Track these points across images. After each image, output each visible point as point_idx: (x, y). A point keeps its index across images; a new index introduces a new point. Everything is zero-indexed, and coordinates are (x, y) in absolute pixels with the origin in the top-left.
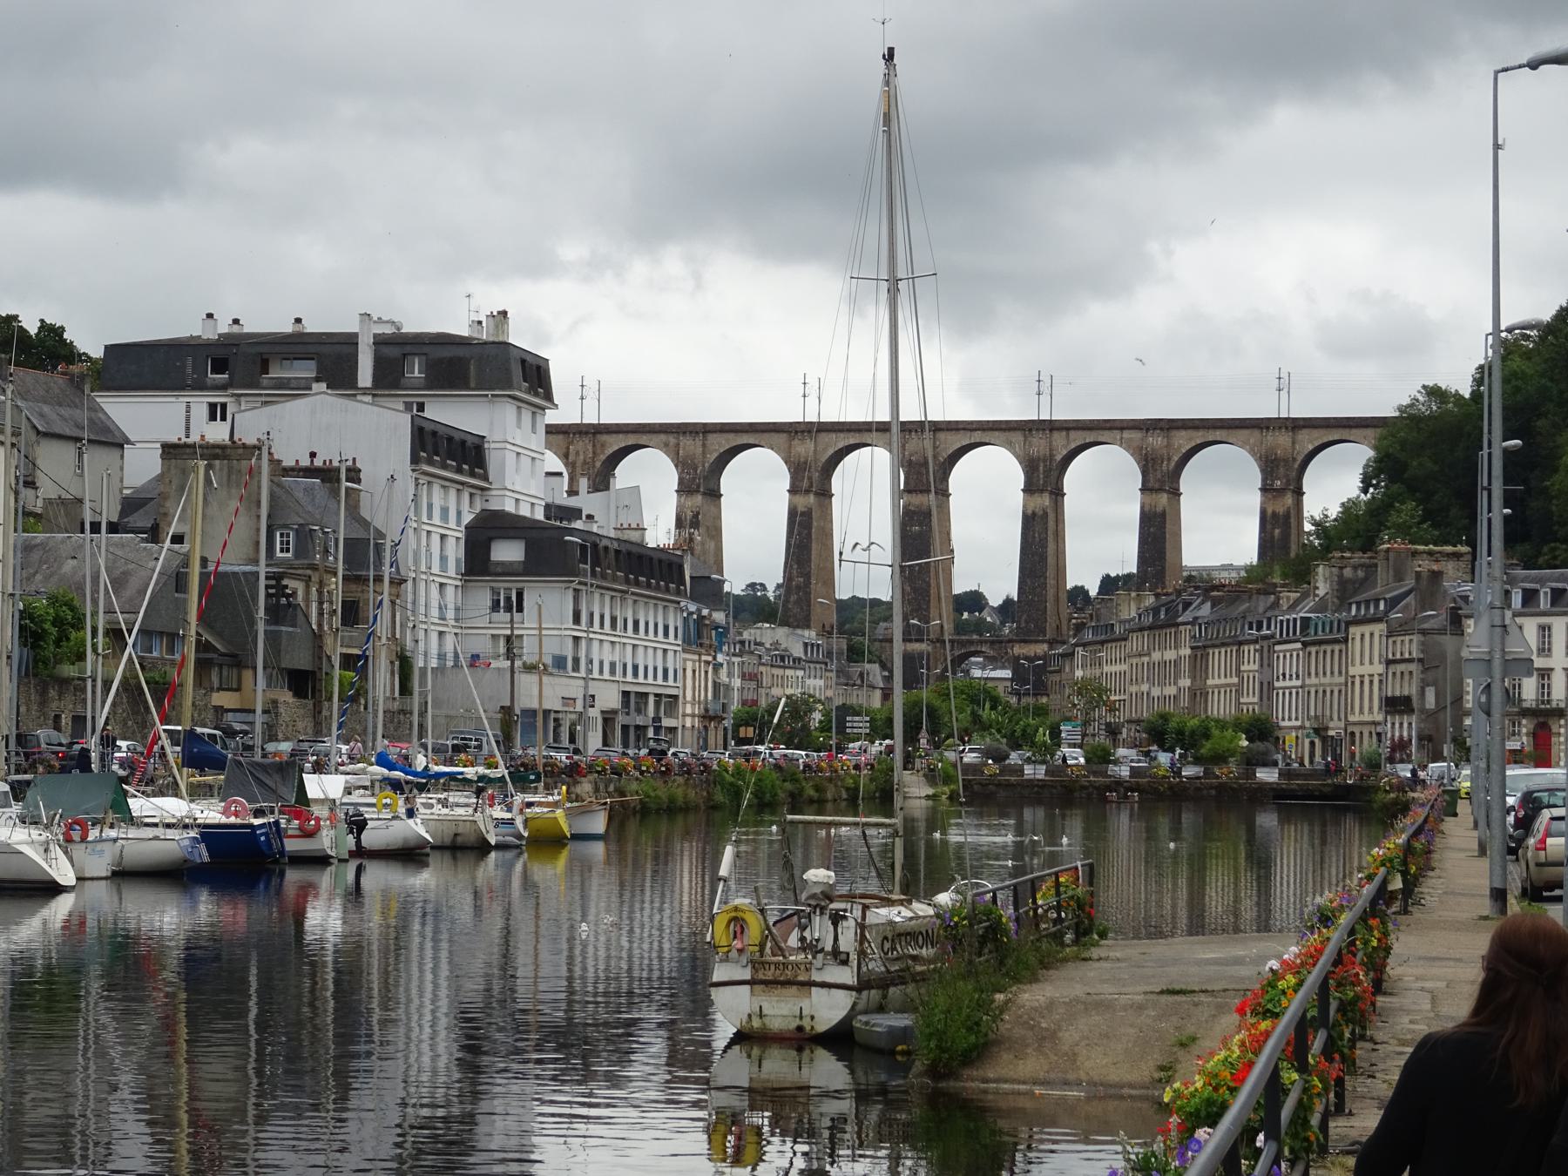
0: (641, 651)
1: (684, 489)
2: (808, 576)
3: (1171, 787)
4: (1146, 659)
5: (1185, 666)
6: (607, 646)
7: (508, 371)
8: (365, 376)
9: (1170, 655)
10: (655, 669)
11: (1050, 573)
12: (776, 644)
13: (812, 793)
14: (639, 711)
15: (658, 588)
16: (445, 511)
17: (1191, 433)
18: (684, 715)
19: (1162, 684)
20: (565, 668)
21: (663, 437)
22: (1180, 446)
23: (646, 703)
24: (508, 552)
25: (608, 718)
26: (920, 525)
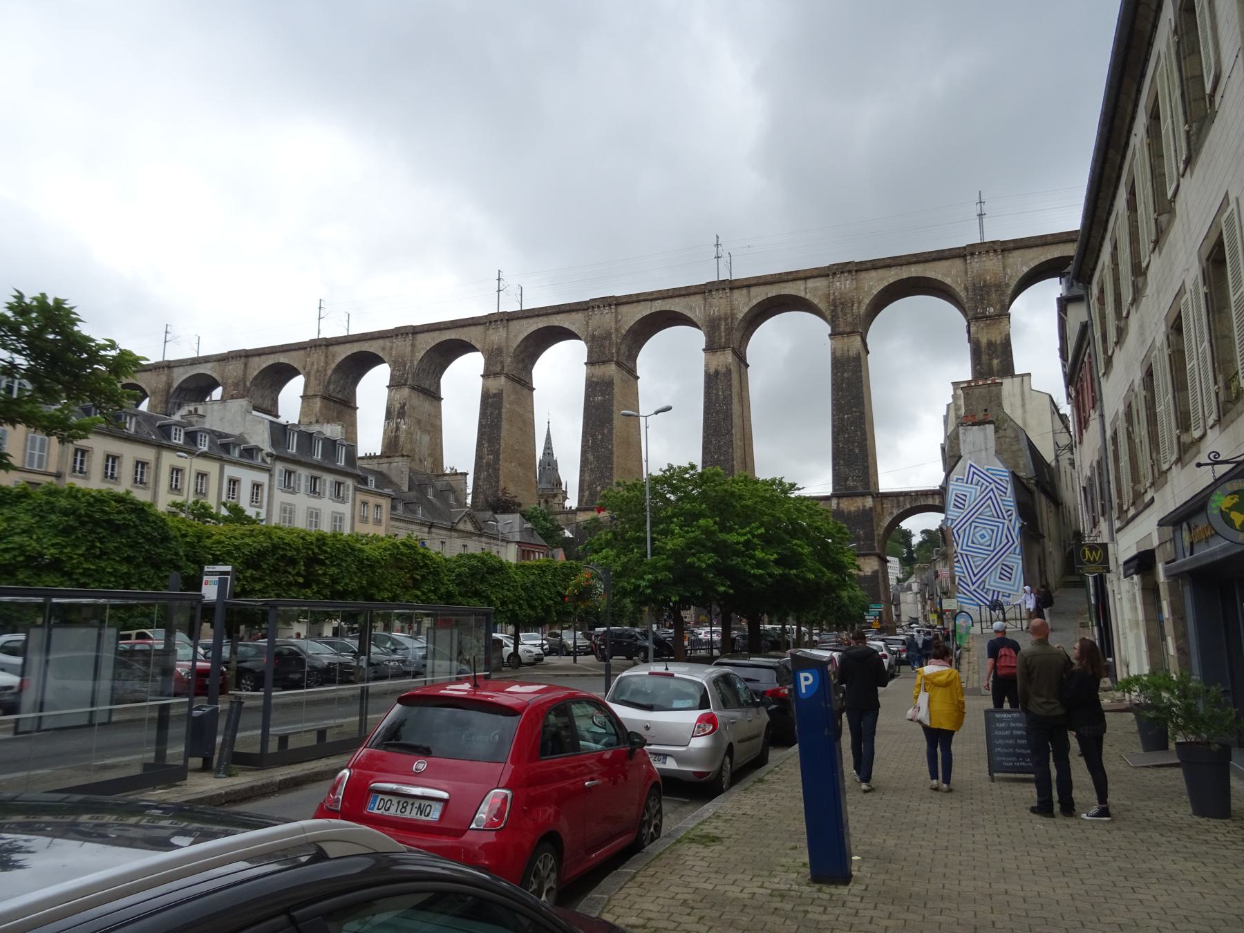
2: (496, 453)
11: (736, 431)
17: (880, 271)
22: (871, 288)
26: (603, 395)
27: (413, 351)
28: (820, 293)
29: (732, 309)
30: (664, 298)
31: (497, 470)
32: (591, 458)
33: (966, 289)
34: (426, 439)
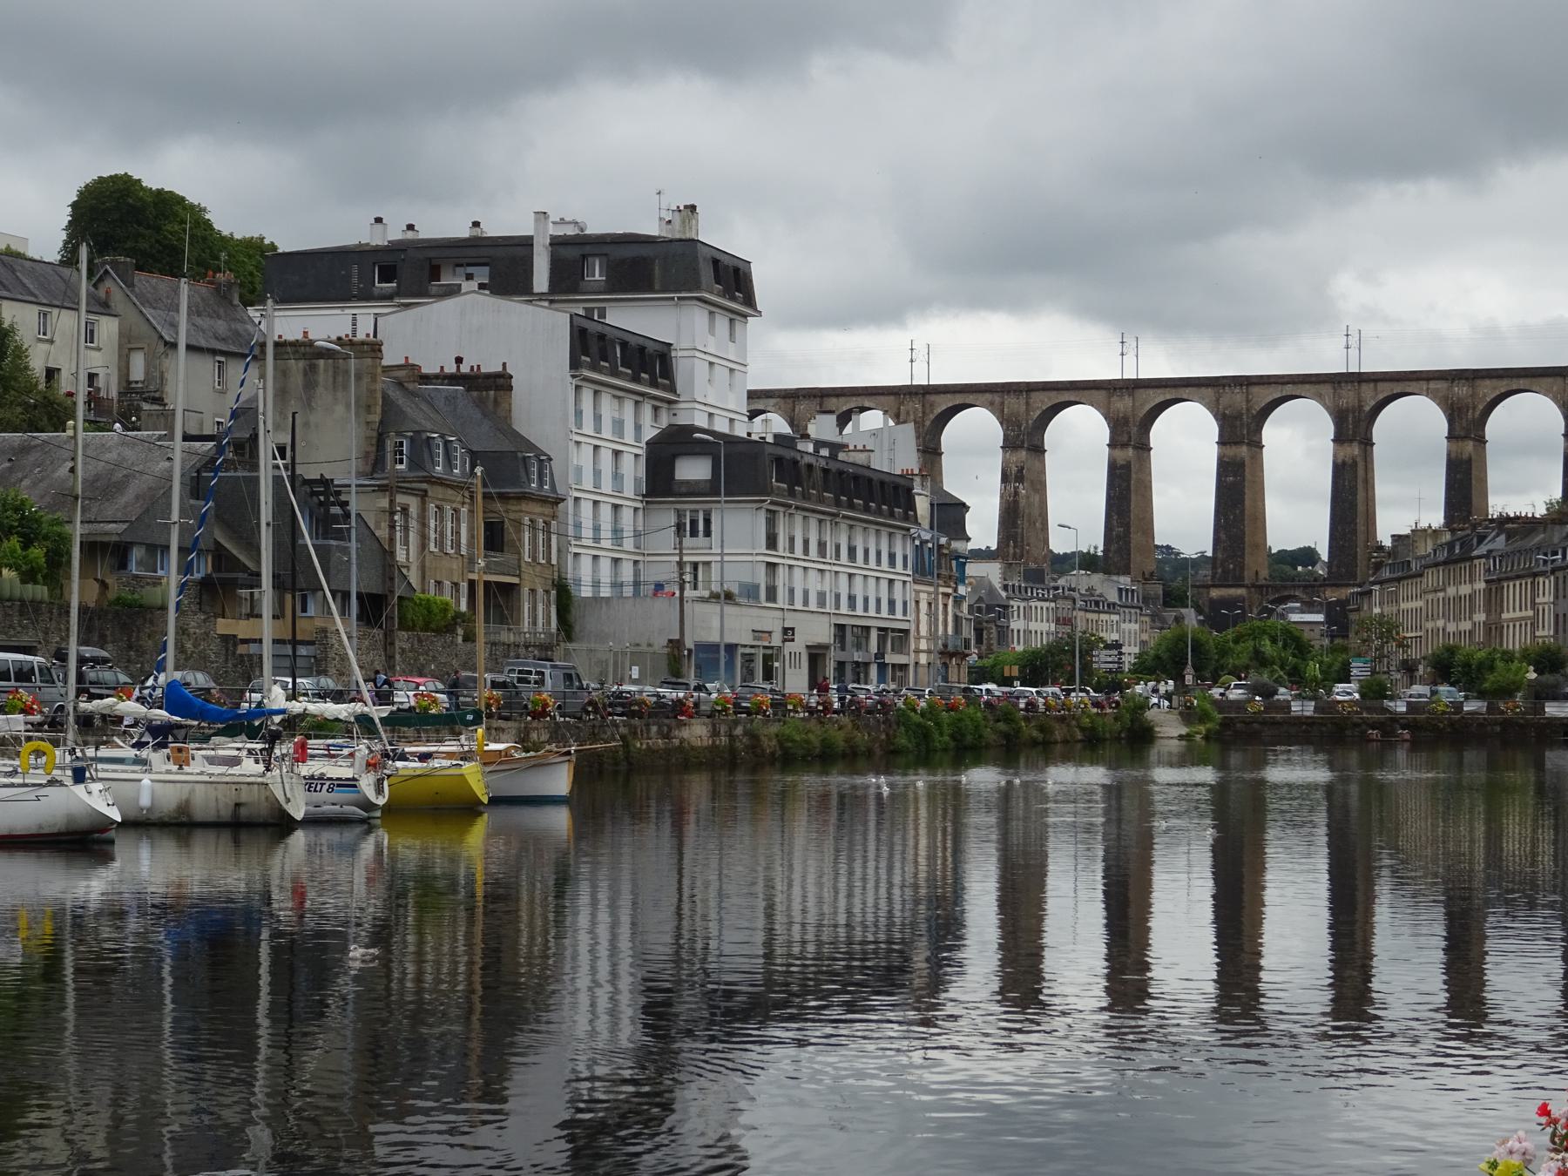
0: (858, 581)
1: (1009, 445)
2: (1127, 526)
3: (1452, 724)
4: (1441, 595)
5: (1480, 601)
6: (812, 575)
7: (696, 271)
8: (541, 281)
9: (1465, 590)
10: (878, 601)
11: (1360, 520)
12: (1090, 589)
13: (1035, 733)
14: (858, 647)
15: (879, 513)
16: (618, 425)
17: (1495, 382)
18: (917, 651)
19: (1458, 619)
20: (757, 598)
21: (988, 396)
23: (868, 638)
24: (693, 470)
25: (816, 656)
27: (1027, 410)
30: (1294, 383)
31: (1128, 543)
32: (1223, 536)
34: (1037, 498)
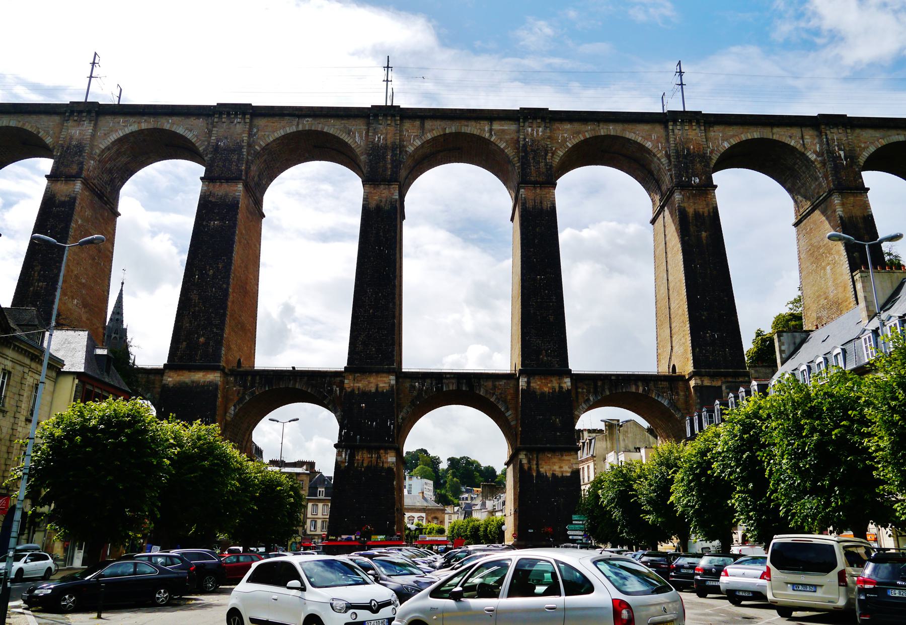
17: (577, 126)
22: (565, 140)
28: (508, 137)
29: (401, 140)
32: (195, 297)
33: (668, 156)
